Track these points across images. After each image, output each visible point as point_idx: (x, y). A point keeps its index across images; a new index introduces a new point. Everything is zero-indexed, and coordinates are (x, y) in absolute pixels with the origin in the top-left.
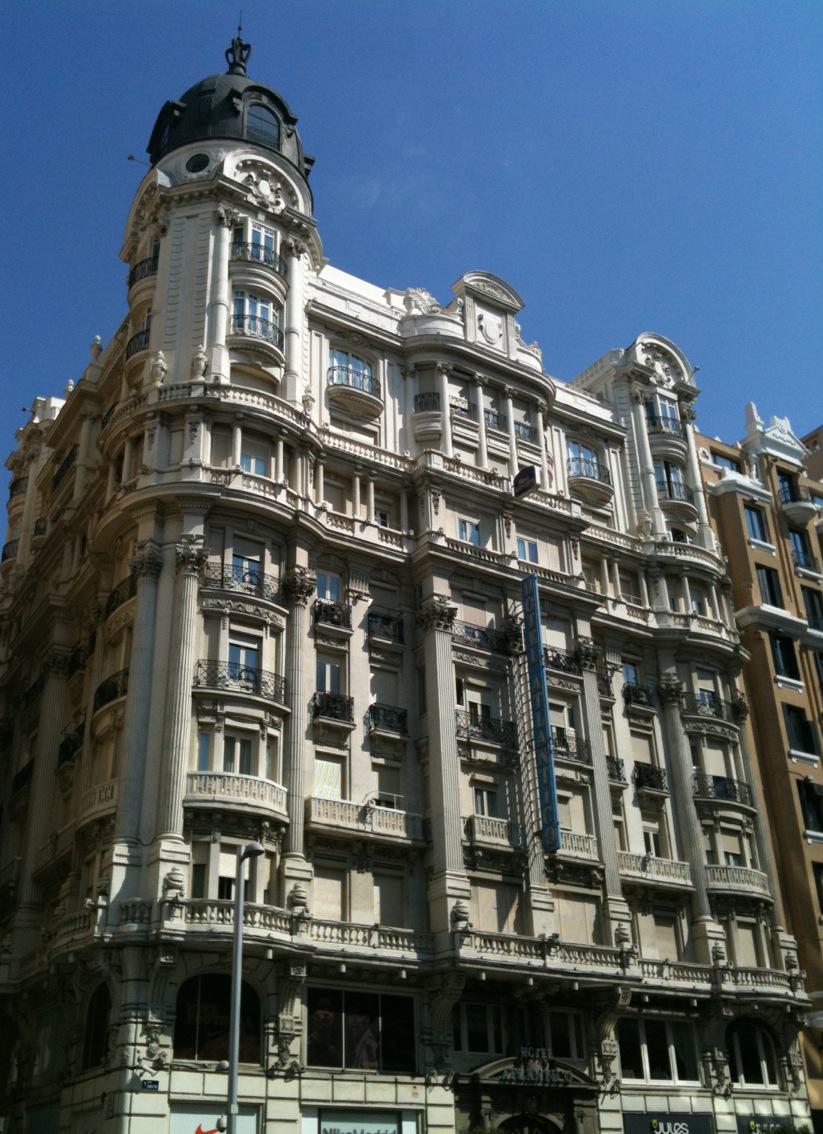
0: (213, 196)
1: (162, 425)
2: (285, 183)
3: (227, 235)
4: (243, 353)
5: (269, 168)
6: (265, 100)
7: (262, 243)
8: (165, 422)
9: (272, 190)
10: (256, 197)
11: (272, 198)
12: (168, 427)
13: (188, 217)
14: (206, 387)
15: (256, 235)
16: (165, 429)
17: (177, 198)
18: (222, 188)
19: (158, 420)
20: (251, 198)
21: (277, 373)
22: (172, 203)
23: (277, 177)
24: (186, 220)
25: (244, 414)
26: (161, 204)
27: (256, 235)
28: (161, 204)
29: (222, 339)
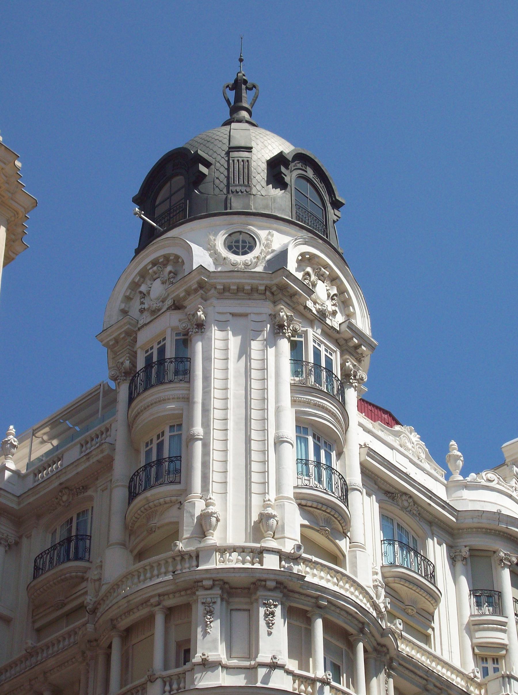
0: (268, 293)
1: (222, 599)
2: (342, 291)
3: (284, 345)
4: (309, 512)
5: (327, 266)
6: (310, 173)
7: (323, 364)
8: (225, 596)
9: (329, 295)
10: (315, 303)
11: (329, 306)
12: (228, 603)
13: (233, 315)
14: (282, 556)
15: (317, 354)
16: (224, 603)
17: (220, 287)
18: (283, 288)
19: (217, 591)
20: (310, 304)
21: (343, 544)
22: (213, 291)
23: (333, 279)
24: (230, 317)
25: (329, 601)
26: (196, 291)
27: (317, 354)
28: (196, 291)
29: (289, 492)
